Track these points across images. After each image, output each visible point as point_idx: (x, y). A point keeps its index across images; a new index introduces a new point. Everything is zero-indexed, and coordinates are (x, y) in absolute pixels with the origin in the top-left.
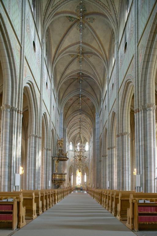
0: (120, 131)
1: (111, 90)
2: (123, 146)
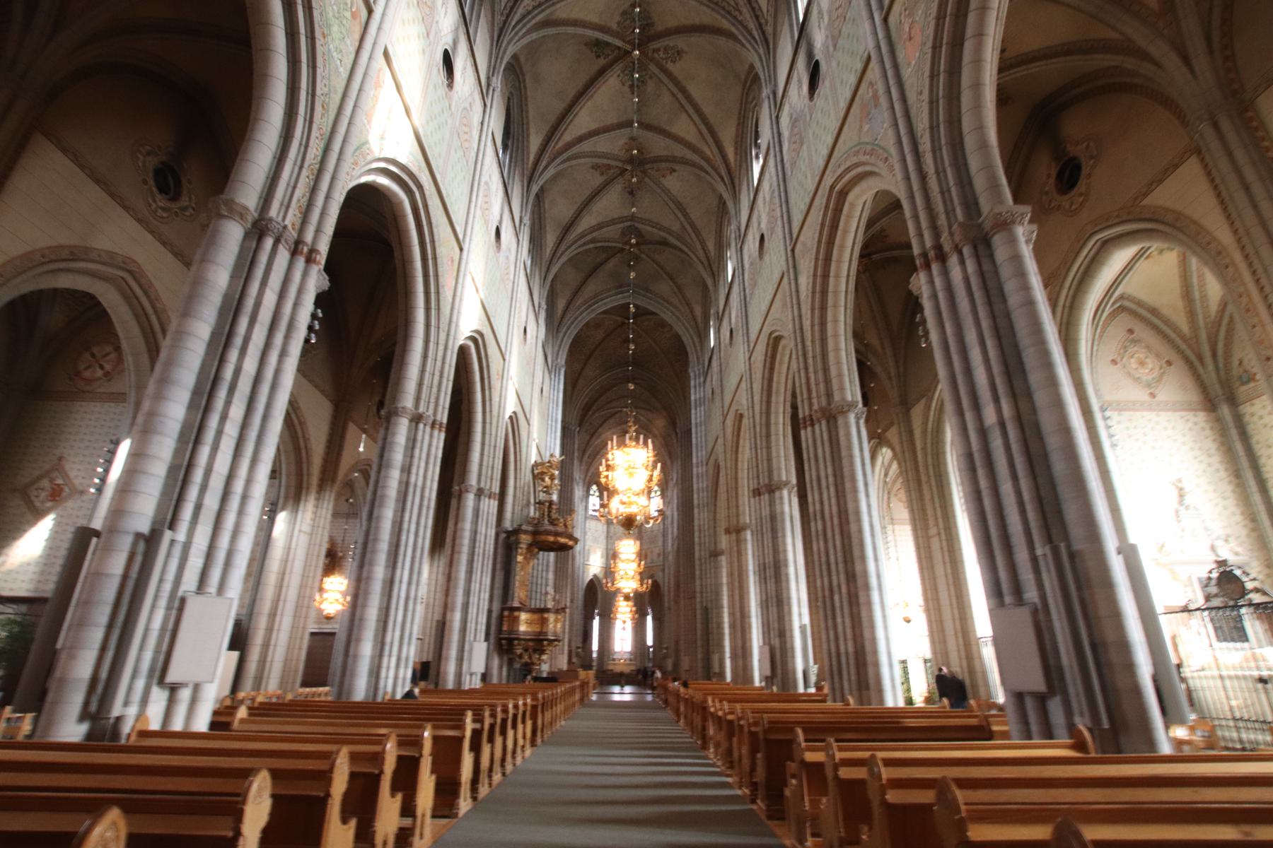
0: (815, 401)
1: (752, 264)
2: (841, 469)
